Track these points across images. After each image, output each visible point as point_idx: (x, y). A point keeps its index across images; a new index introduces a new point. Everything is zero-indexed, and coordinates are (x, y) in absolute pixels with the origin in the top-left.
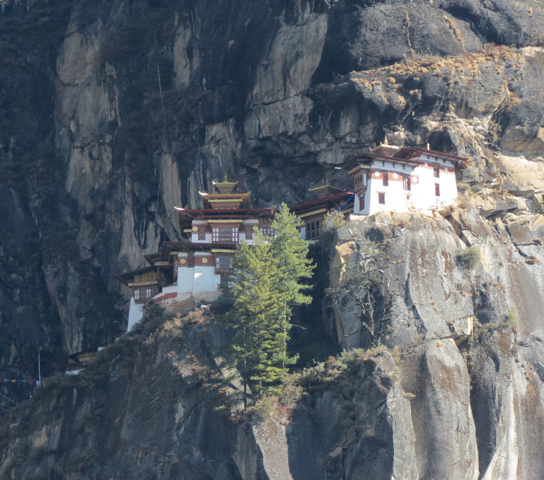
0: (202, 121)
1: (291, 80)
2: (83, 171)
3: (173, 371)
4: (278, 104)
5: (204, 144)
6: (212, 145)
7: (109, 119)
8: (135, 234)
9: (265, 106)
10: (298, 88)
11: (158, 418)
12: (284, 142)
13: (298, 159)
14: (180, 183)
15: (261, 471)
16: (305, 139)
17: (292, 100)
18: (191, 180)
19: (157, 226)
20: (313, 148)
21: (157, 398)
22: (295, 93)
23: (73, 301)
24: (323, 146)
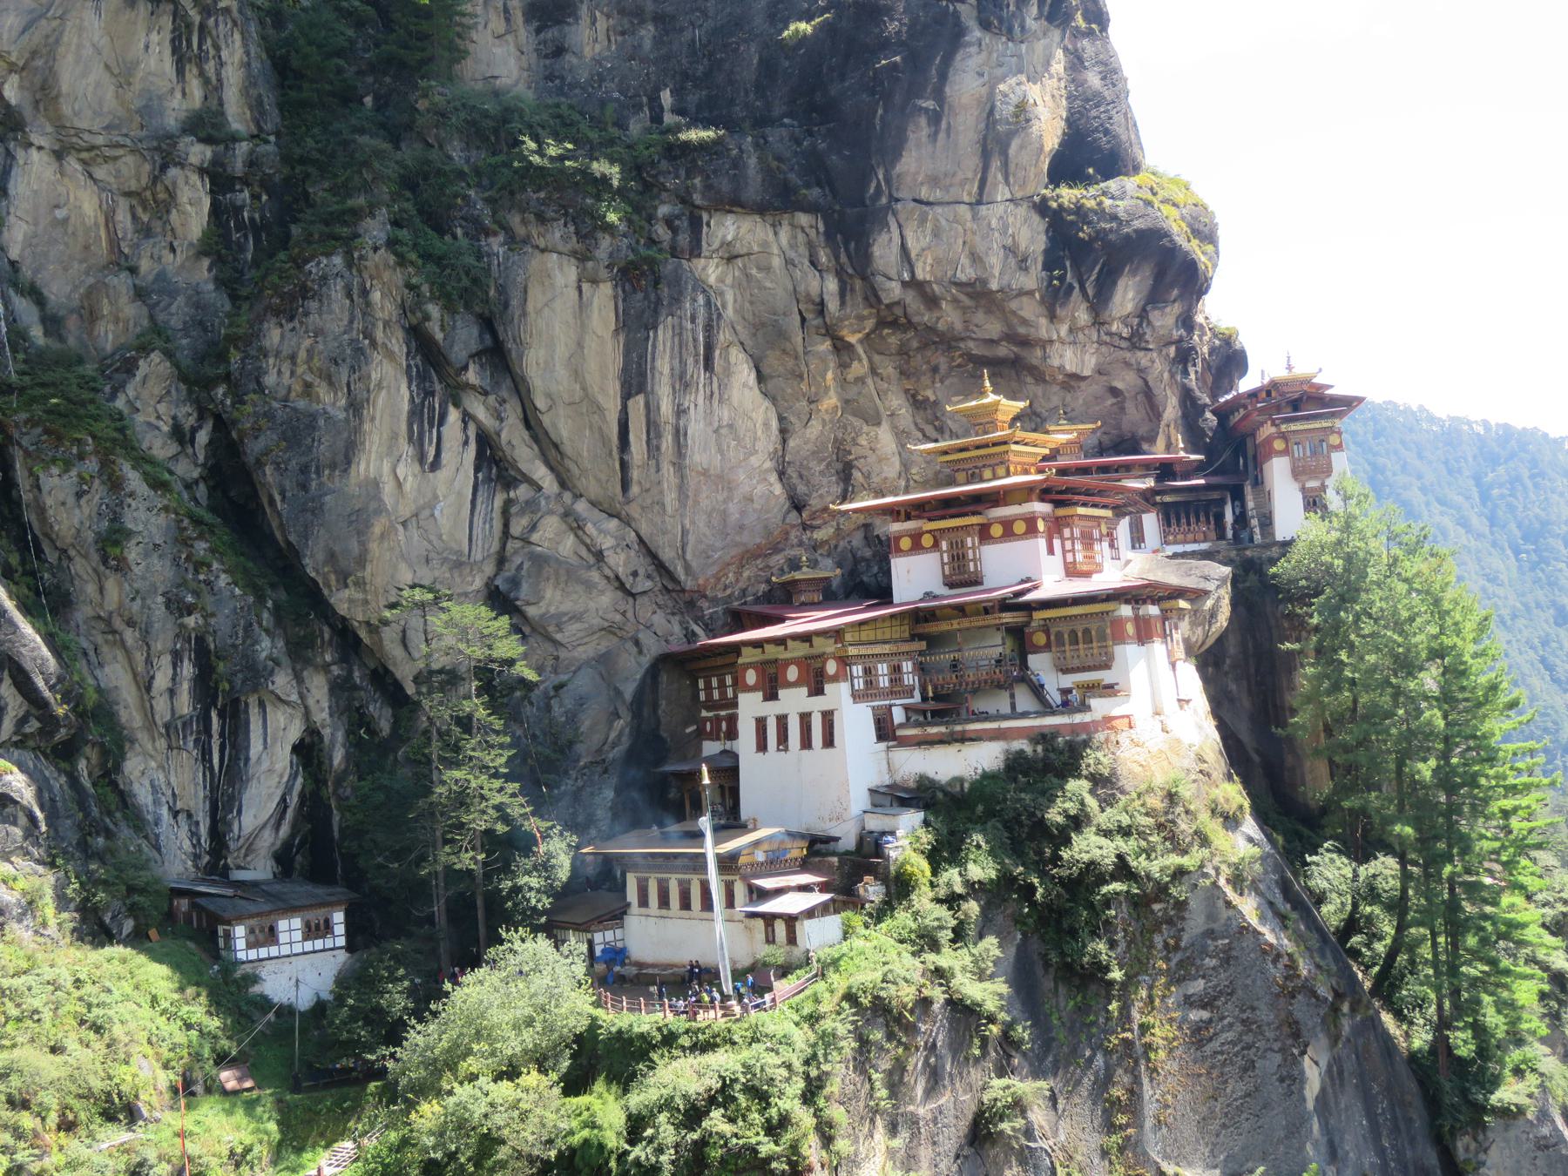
1: (1005, 164)
2: (60, 214)
4: (963, 209)
5: (699, 256)
7: (181, 103)
10: (1023, 185)
11: (1248, 1095)
12: (955, 301)
13: (971, 344)
14: (622, 339)
16: (1029, 309)
17: (999, 209)
18: (660, 337)
19: (467, 417)
20: (1043, 328)
21: (1230, 1036)
22: (1008, 196)
23: (151, 567)
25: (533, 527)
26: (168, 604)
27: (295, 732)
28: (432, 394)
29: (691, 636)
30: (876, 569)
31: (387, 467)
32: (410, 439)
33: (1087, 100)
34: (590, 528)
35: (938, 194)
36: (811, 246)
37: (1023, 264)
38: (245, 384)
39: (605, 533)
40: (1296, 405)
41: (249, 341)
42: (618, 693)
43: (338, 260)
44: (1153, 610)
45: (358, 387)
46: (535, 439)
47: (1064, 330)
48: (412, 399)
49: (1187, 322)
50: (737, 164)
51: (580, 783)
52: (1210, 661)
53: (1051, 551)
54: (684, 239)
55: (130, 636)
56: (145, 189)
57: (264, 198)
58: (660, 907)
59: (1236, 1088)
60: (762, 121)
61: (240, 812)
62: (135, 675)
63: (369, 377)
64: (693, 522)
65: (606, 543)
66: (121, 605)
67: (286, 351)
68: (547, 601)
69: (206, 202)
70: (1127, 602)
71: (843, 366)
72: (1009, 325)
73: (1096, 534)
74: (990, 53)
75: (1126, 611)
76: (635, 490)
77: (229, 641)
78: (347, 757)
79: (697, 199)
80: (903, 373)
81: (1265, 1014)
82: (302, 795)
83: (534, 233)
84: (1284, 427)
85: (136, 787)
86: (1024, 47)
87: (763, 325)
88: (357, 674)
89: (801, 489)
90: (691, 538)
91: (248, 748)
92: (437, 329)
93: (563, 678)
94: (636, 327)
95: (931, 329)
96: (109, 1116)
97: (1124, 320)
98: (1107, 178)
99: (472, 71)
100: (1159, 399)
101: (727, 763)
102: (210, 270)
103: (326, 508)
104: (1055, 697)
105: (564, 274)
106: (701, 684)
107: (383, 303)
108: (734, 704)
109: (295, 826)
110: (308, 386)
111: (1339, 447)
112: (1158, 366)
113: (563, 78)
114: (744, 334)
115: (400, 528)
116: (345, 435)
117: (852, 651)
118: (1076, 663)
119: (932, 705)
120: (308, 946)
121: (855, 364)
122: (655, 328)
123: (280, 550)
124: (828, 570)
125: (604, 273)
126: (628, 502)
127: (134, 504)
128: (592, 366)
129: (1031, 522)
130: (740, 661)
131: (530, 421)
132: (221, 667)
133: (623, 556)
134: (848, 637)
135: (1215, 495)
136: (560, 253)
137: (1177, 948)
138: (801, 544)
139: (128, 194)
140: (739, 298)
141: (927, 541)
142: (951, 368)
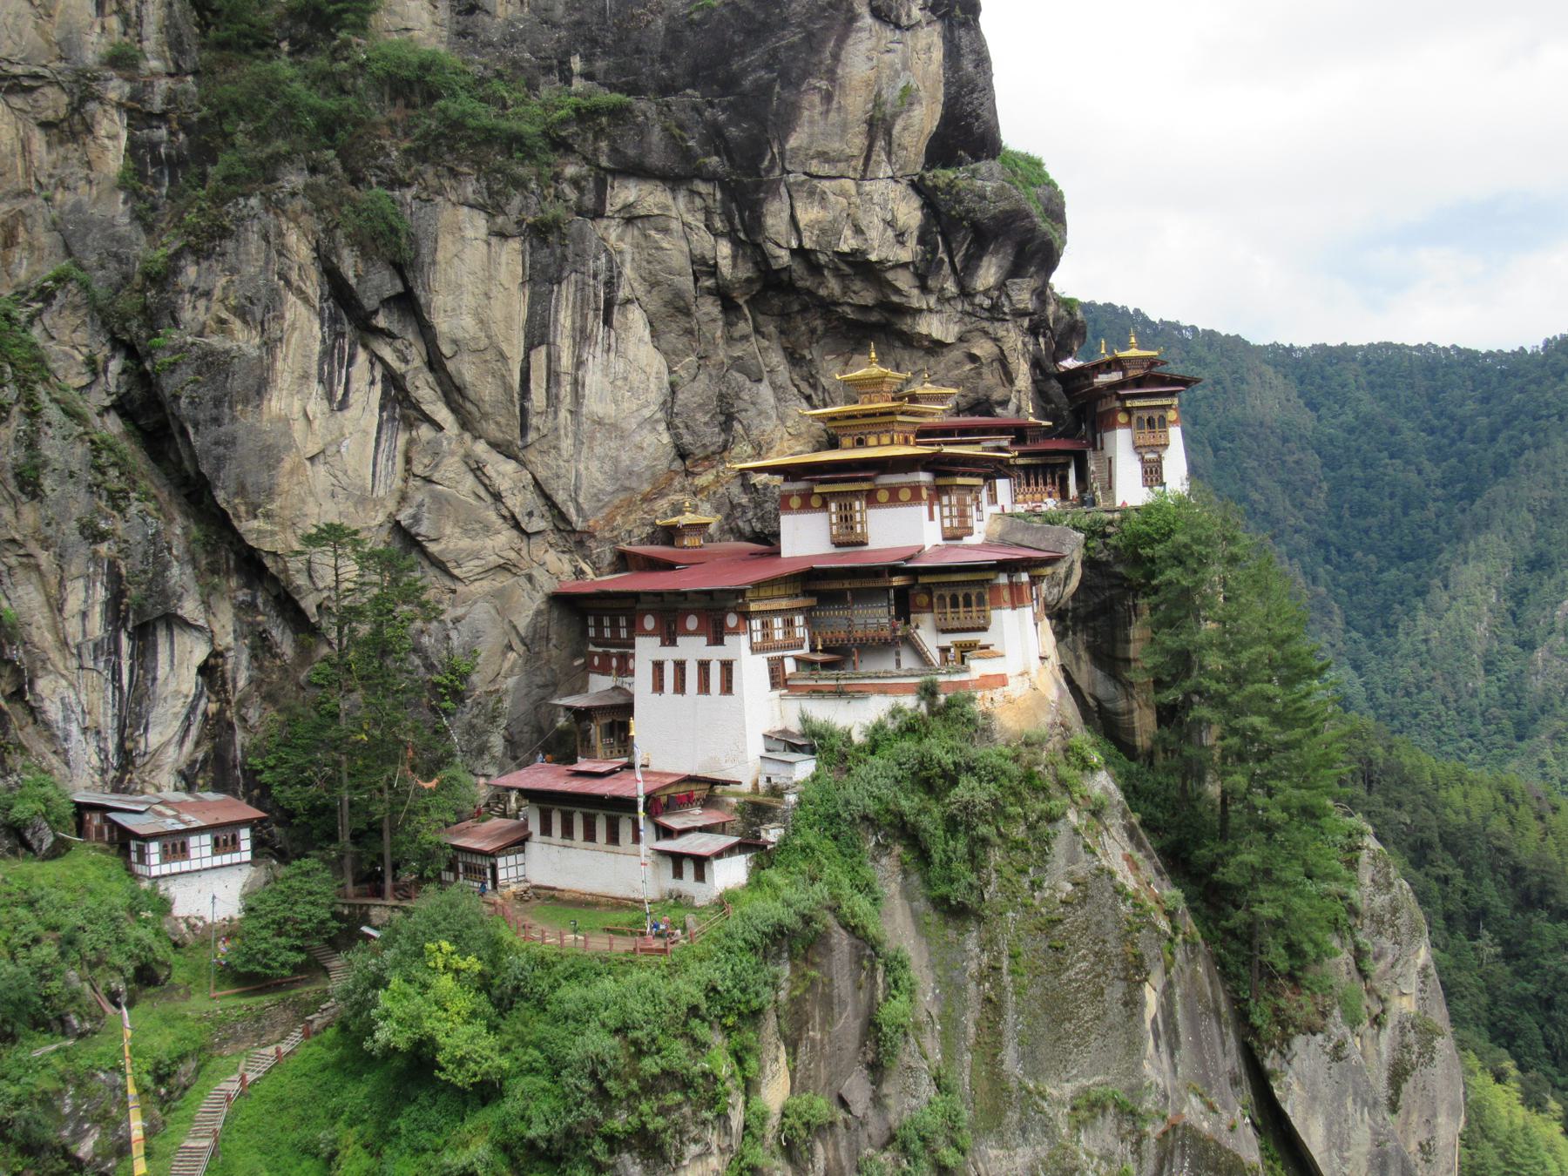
0: (604, 162)
1: (890, 144)
3: (1124, 901)
4: (849, 185)
6: (613, 223)
8: (321, 369)
9: (815, 182)
11: (1098, 1018)
12: (837, 272)
13: (848, 309)
15: (1389, 1145)
16: (904, 281)
19: (375, 358)
20: (916, 300)
21: (1084, 965)
24: (932, 301)
25: (436, 465)
26: (83, 528)
27: (200, 653)
28: (343, 335)
29: (579, 573)
30: (750, 515)
31: (297, 405)
32: (321, 381)
33: (961, 87)
34: (489, 470)
35: (826, 169)
36: (708, 212)
37: (900, 237)
38: (158, 315)
39: (503, 471)
40: (1138, 382)
41: (161, 278)
42: (515, 627)
43: (253, 202)
44: (1025, 577)
45: (274, 330)
46: (440, 384)
47: (932, 301)
48: (323, 341)
49: (1042, 293)
50: (642, 130)
51: (475, 711)
52: (1062, 619)
53: (931, 518)
54: (589, 201)
55: (45, 558)
56: (62, 121)
57: (181, 136)
58: (563, 837)
59: (1088, 1012)
60: (666, 89)
61: (146, 729)
62: (48, 597)
63: (282, 317)
64: (587, 468)
65: (503, 485)
66: (37, 530)
67: (202, 286)
68: (449, 541)
69: (124, 135)
70: (1004, 571)
71: (729, 324)
72: (887, 296)
73: (969, 500)
74: (879, 39)
75: (1003, 579)
76: (532, 436)
77: (141, 567)
78: (251, 681)
79: (604, 162)
80: (782, 332)
81: (1112, 946)
82: (205, 714)
83: (447, 183)
84: (1128, 404)
85: (47, 704)
86: (908, 34)
87: (658, 283)
88: (260, 601)
89: (687, 439)
90: (585, 484)
91: (155, 668)
92: (351, 274)
93: (460, 611)
94: (541, 281)
95: (809, 292)
96: (40, 1024)
97: (986, 293)
98: (978, 159)
99: (381, 21)
100: (1012, 367)
101: (620, 700)
102: (125, 202)
103: (239, 441)
104: (935, 656)
105: (476, 225)
106: (591, 621)
107: (300, 248)
108: (633, 646)
109: (197, 744)
110: (222, 321)
111: (1174, 423)
112: (1012, 334)
113: (475, 35)
114: (640, 290)
115: (308, 463)
116: (258, 372)
117: (753, 607)
118: (956, 624)
119: (819, 657)
120: (217, 861)
121: (742, 324)
122: (560, 283)
123: (188, 477)
124: (707, 515)
125: (511, 229)
126: (525, 447)
127: (50, 432)
128: (497, 312)
129: (915, 490)
130: (638, 607)
131: (435, 363)
132: (133, 592)
133: (519, 498)
134: (748, 594)
135: (1061, 460)
136: (471, 206)
137: (1040, 887)
138: (683, 490)
139: (45, 125)
140: (637, 256)
141: (815, 502)
142: (826, 331)
